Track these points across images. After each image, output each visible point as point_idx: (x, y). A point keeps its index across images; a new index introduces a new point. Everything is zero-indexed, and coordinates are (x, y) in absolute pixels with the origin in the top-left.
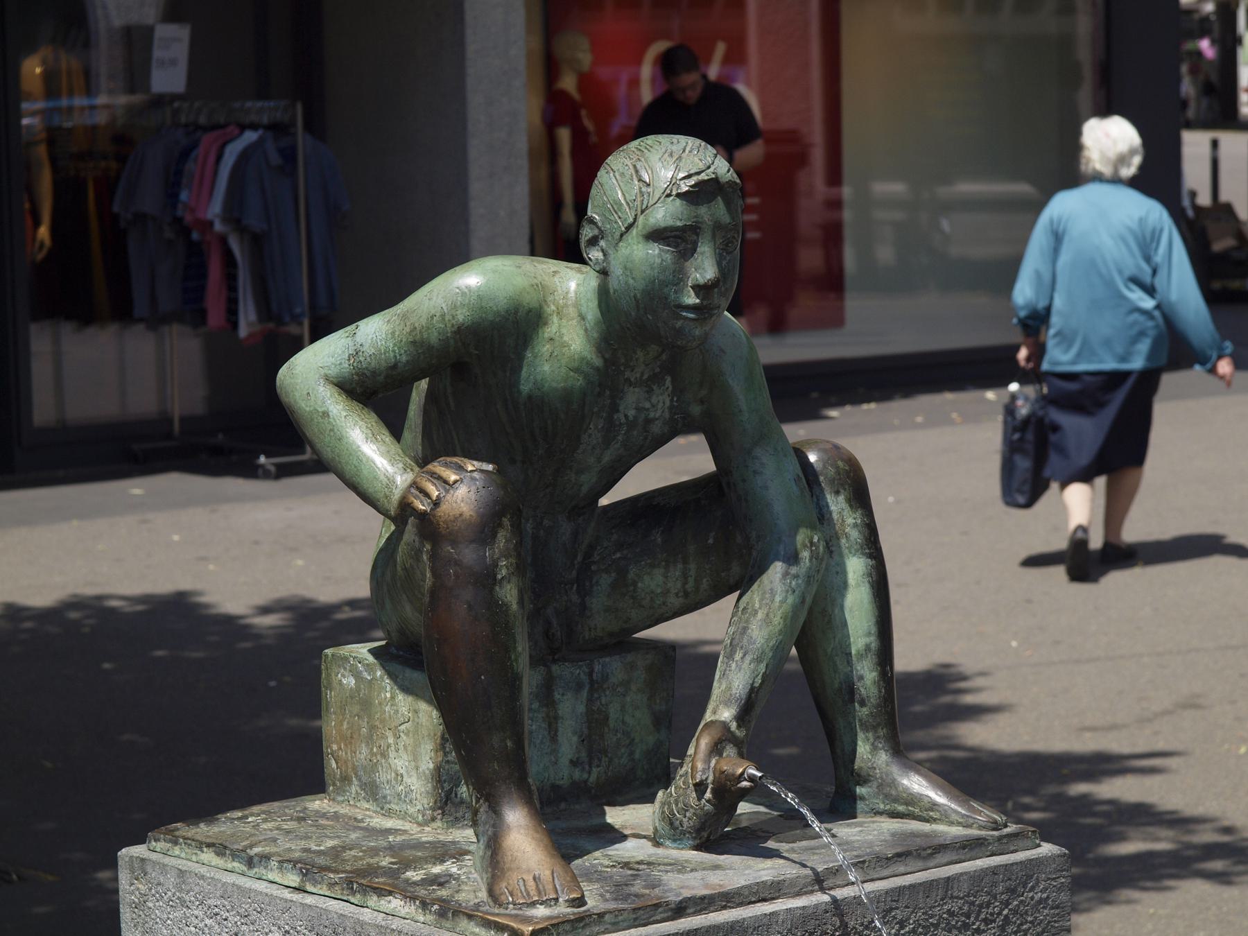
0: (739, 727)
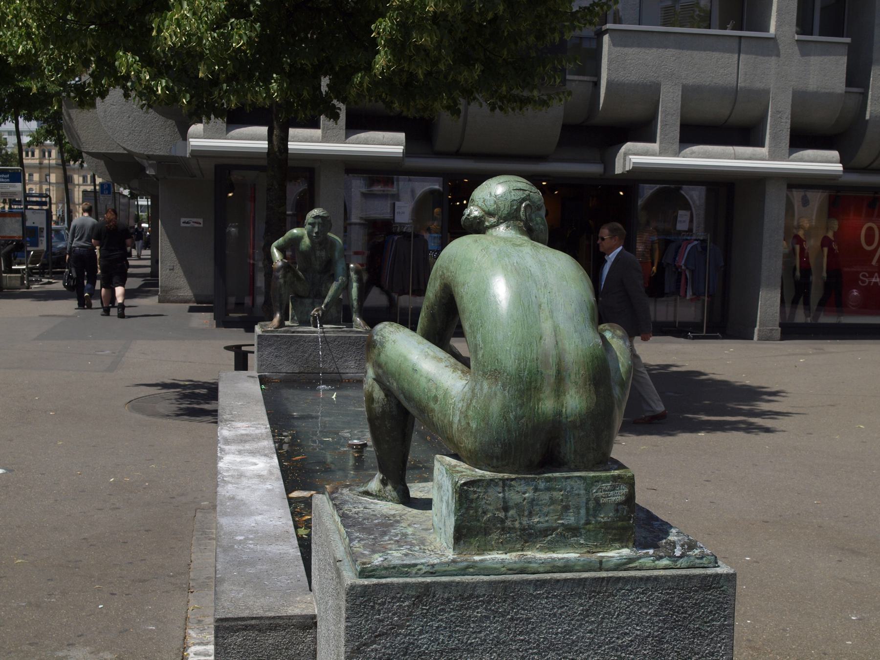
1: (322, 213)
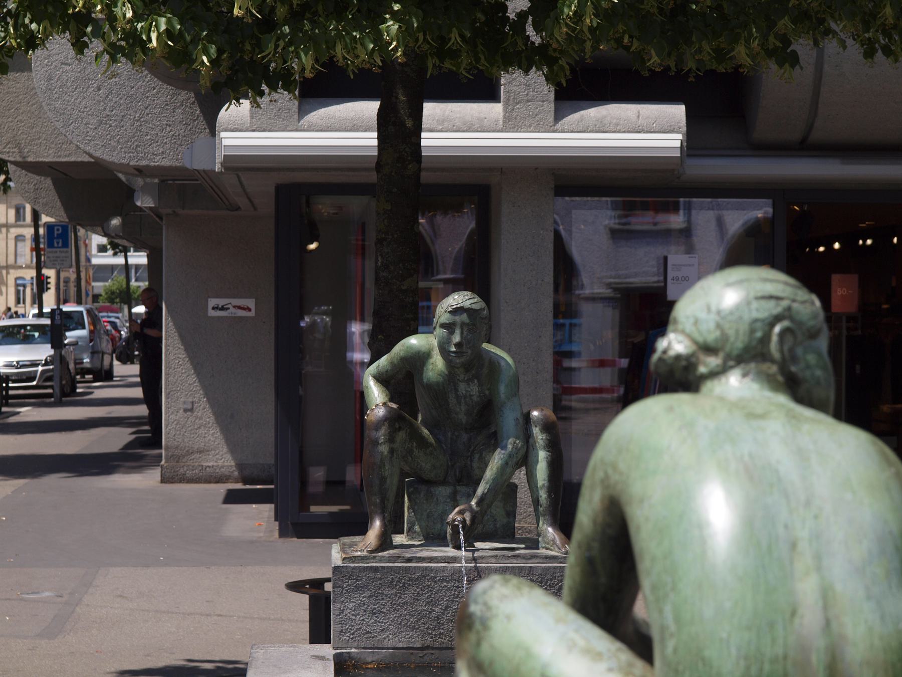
0: (476, 506)
1: (469, 302)
